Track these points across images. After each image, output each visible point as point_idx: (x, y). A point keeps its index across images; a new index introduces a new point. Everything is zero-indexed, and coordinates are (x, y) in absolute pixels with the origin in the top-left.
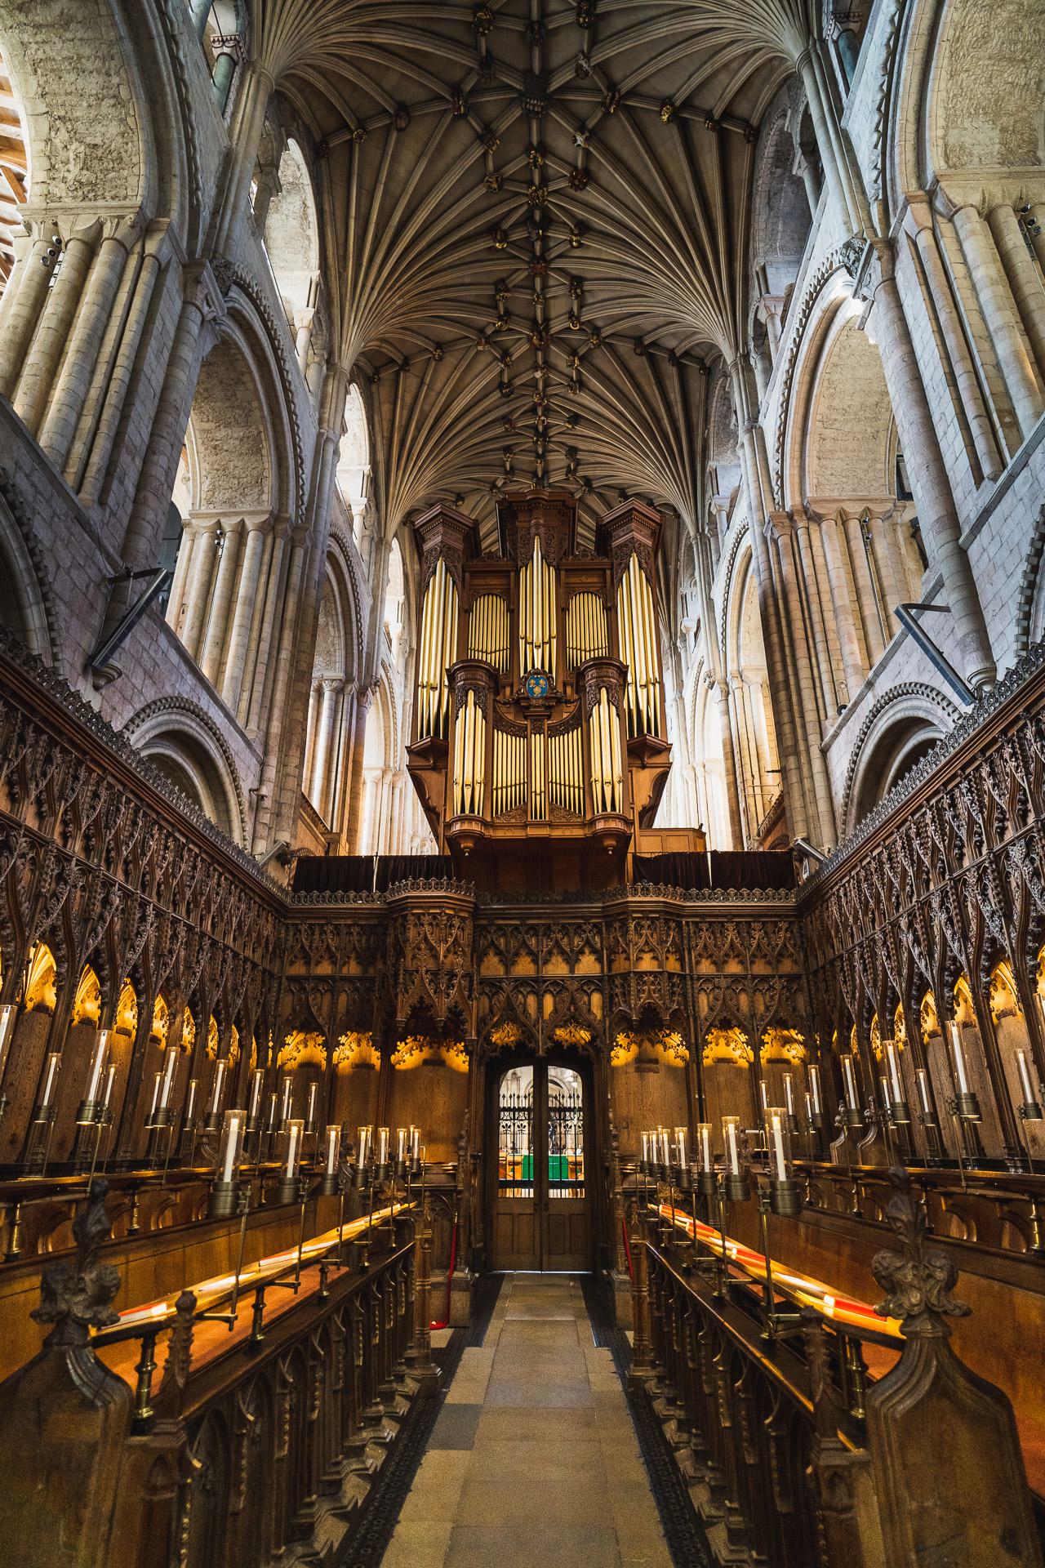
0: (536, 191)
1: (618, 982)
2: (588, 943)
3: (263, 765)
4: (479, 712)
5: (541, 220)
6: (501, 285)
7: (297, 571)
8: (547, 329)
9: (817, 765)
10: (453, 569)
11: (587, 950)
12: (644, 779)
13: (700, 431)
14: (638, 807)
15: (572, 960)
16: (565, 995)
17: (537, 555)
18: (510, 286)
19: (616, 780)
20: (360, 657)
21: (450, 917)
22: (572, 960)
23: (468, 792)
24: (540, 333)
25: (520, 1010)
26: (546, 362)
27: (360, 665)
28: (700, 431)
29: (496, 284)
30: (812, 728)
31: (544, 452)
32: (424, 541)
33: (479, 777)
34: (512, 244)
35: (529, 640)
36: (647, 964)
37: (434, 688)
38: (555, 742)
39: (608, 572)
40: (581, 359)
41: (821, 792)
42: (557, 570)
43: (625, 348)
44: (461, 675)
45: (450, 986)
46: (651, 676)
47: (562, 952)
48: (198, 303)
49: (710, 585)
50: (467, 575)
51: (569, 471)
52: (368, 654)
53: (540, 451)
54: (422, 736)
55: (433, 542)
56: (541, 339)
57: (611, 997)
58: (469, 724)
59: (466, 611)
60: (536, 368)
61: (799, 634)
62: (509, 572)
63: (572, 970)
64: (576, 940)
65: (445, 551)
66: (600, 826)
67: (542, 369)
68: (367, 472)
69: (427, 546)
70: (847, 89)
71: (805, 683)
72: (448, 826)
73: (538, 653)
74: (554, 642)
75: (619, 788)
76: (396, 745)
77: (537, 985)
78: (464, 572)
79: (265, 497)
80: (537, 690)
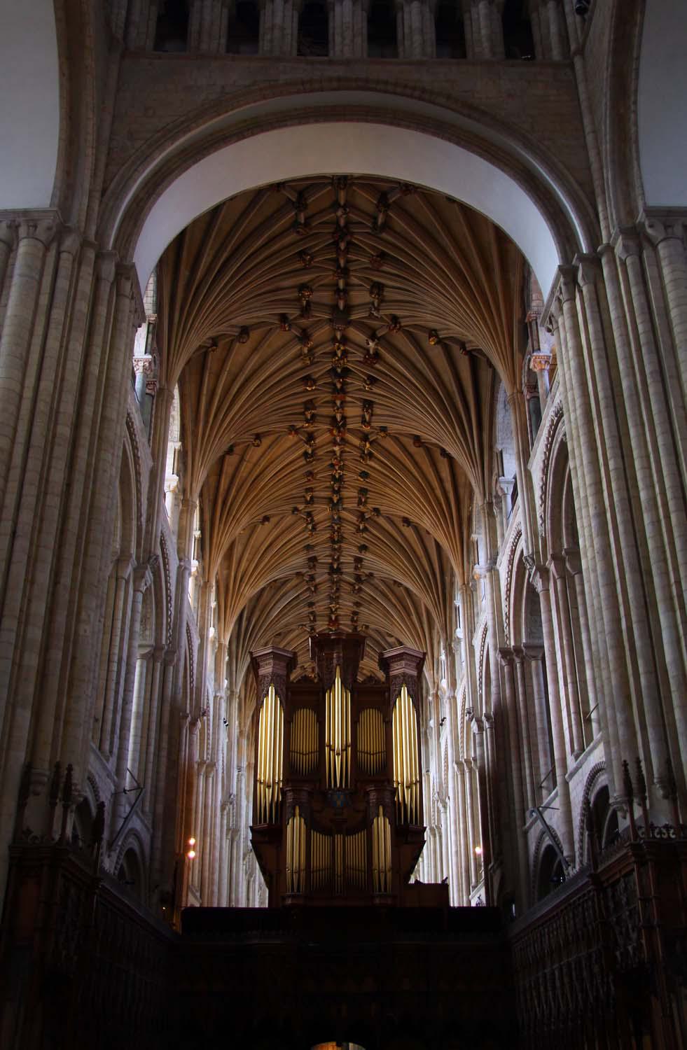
0: (338, 360)
3: (153, 838)
4: (303, 820)
5: (341, 339)
6: (309, 405)
7: (170, 685)
8: (344, 425)
13: (466, 506)
17: (338, 682)
18: (316, 405)
19: (387, 869)
24: (338, 428)
26: (342, 439)
27: (191, 700)
28: (466, 506)
29: (305, 403)
31: (339, 489)
32: (259, 667)
33: (303, 867)
34: (319, 385)
35: (332, 748)
37: (269, 787)
38: (349, 839)
39: (387, 694)
40: (371, 443)
43: (409, 442)
44: (289, 794)
46: (414, 779)
48: (141, 589)
49: (472, 633)
50: (289, 694)
51: (360, 503)
52: (197, 688)
53: (336, 489)
54: (260, 822)
55: (267, 669)
56: (339, 432)
58: (295, 828)
59: (288, 722)
60: (335, 443)
65: (275, 679)
66: (377, 901)
67: (339, 445)
68: (177, 448)
69: (262, 672)
70: (533, 444)
71: (515, 781)
72: (284, 899)
73: (338, 759)
75: (389, 875)
76: (208, 739)
79: (147, 633)
80: (339, 803)
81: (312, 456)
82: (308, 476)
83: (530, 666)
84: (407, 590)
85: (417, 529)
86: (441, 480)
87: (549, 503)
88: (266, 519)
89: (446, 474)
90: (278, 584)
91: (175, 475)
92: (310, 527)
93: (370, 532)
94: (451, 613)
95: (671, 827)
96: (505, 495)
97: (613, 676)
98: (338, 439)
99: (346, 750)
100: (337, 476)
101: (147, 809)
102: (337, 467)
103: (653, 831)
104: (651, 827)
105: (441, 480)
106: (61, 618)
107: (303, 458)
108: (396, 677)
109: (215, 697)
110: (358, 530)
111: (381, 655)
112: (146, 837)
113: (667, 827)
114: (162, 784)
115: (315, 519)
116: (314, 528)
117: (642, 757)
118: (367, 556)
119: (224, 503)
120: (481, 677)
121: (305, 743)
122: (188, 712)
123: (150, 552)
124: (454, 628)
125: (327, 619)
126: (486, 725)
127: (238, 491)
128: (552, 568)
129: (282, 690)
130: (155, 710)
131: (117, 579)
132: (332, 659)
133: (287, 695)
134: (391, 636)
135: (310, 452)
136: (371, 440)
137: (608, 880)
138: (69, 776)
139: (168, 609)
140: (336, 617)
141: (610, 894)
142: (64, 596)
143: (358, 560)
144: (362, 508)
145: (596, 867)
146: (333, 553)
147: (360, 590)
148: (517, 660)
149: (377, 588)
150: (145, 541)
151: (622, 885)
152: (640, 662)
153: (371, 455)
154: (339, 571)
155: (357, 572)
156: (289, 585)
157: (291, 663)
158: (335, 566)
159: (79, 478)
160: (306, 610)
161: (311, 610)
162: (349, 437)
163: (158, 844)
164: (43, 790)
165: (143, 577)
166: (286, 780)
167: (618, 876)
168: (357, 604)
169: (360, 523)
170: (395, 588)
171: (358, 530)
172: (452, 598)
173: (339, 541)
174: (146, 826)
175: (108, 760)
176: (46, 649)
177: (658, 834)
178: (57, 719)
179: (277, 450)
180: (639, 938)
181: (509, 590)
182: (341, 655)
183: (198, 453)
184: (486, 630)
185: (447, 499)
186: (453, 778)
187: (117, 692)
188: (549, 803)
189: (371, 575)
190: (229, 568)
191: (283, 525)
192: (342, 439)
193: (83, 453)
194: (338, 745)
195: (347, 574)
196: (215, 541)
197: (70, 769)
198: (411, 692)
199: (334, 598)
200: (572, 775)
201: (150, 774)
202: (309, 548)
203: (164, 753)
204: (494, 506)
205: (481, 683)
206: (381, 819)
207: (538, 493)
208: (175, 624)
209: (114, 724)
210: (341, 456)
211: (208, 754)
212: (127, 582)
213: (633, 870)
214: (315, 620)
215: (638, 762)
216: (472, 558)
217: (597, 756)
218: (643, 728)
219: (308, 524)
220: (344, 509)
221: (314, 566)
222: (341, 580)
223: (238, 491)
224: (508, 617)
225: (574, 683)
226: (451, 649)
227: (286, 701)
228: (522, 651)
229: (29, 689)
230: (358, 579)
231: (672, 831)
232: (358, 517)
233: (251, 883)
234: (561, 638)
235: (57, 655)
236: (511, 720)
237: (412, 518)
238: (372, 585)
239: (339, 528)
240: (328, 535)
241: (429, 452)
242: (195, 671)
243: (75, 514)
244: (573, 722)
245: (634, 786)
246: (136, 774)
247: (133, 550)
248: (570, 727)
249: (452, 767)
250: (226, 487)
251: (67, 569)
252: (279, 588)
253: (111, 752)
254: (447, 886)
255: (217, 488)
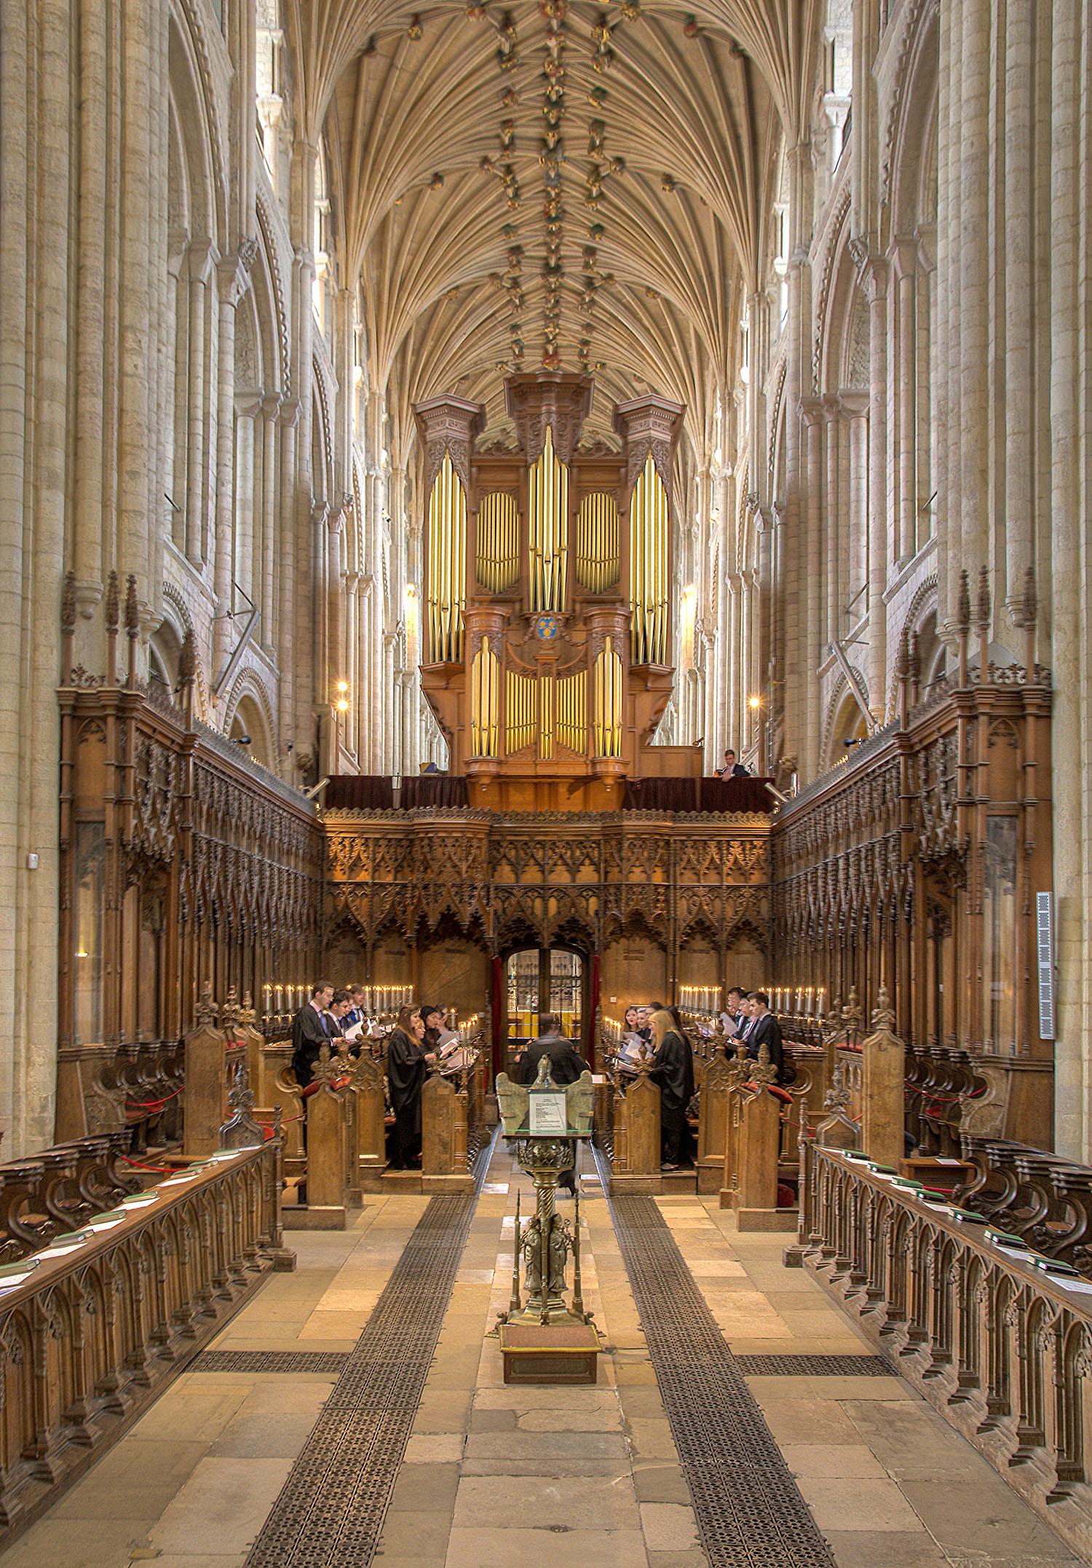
1: (612, 890)
2: (588, 856)
3: (280, 680)
4: (494, 658)
9: (811, 690)
10: (459, 467)
11: (587, 862)
12: (646, 701)
14: (639, 731)
15: (574, 870)
16: (567, 900)
17: (548, 450)
20: (329, 471)
21: (470, 840)
22: (574, 870)
23: (485, 735)
25: (529, 912)
26: (563, 24)
30: (810, 651)
36: (637, 876)
41: (811, 716)
42: (570, 467)
45: (471, 897)
47: (566, 864)
48: (232, 300)
50: (474, 470)
51: (593, 147)
53: (553, 121)
56: (557, 9)
57: (606, 902)
59: (473, 513)
60: (550, 32)
61: (812, 548)
62: (518, 467)
63: (574, 880)
64: (578, 853)
74: (564, 554)
75: (617, 733)
76: (360, 540)
77: (543, 891)
78: (471, 466)
81: (509, 60)
82: (505, 97)
83: (848, 427)
84: (667, 302)
85: (685, 195)
86: (728, 104)
87: (901, 141)
88: (438, 178)
89: (737, 91)
90: (461, 294)
91: (276, 96)
92: (510, 192)
93: (611, 203)
94: (734, 342)
95: (1021, 669)
96: (831, 127)
97: (964, 439)
98: (555, 23)
99: (559, 555)
100: (554, 98)
101: (269, 642)
102: (553, 80)
103: (992, 674)
104: (992, 667)
105: (728, 104)
106: (93, 344)
107: (495, 62)
108: (637, 443)
109: (368, 477)
110: (590, 198)
111: (616, 407)
112: (269, 681)
113: (1014, 668)
114: (289, 606)
115: (518, 178)
116: (516, 195)
117: (991, 565)
118: (602, 243)
119: (366, 147)
120: (773, 445)
121: (500, 543)
122: (325, 499)
123: (241, 236)
124: (737, 367)
125: (541, 352)
126: (777, 520)
127: (388, 126)
128: (894, 260)
129: (462, 463)
130: (271, 496)
131: (191, 283)
132: (539, 415)
133: (470, 473)
134: (640, 380)
135: (506, 49)
136: (611, 24)
137: (921, 741)
138: (131, 590)
139: (280, 335)
140: (556, 348)
141: (922, 761)
142: (94, 308)
143: (590, 251)
144: (596, 157)
145: (907, 724)
146: (548, 239)
147: (593, 301)
148: (828, 417)
149: (619, 301)
150: (230, 215)
151: (940, 747)
152: (1009, 415)
153: (610, 53)
154: (557, 270)
155: (588, 273)
156: (479, 296)
157: (477, 422)
158: (553, 263)
159: (93, 92)
160: (509, 337)
161: (514, 337)
162: (574, 19)
163: (288, 689)
164: (98, 612)
165: (232, 279)
166: (471, 601)
167: (935, 737)
168: (589, 327)
169: (593, 184)
170: (649, 300)
171: (590, 198)
172: (737, 318)
173: (557, 219)
174: (268, 666)
175: (200, 571)
176: (75, 395)
177: (1000, 677)
178: (105, 505)
179: (449, 46)
180: (953, 817)
181: (824, 301)
182: (554, 408)
183: (313, 51)
184: (784, 368)
185: (736, 138)
186: (724, 598)
187: (205, 467)
188: (856, 635)
189: (610, 277)
190: (381, 265)
191: (465, 191)
192: (563, 24)
193: (94, 44)
194: (548, 548)
195: (571, 275)
196: (353, 217)
197: (132, 581)
198: (661, 468)
199: (551, 318)
200: (892, 594)
201: (270, 590)
202: (508, 229)
203: (289, 560)
204: (813, 151)
205: (772, 454)
206: (609, 655)
207: (884, 121)
208: (294, 359)
209: (205, 516)
210: (560, 57)
211: (360, 562)
212: (207, 288)
213: (956, 728)
214: (521, 355)
215: (984, 573)
216: (771, 246)
217: (928, 568)
218: (1000, 520)
219: (508, 186)
220: (565, 159)
221: (519, 262)
222: (561, 286)
223: (388, 126)
224: (819, 346)
225: (911, 452)
226: (731, 400)
227: (470, 480)
228: (837, 402)
229: (58, 460)
230: (589, 283)
231: (1021, 673)
232: (590, 174)
233: (435, 745)
234: (896, 380)
235: (93, 405)
236: (812, 512)
237: (679, 176)
238: (612, 294)
239: (558, 195)
240: (540, 208)
241: (709, 45)
242: (332, 436)
243: (95, 162)
244: (902, 515)
245: (974, 608)
246: (248, 590)
247: (212, 233)
248: (897, 521)
249: (723, 584)
250: (367, 120)
251: (95, 260)
252: (462, 302)
253: (204, 558)
254: (702, 748)
255: (353, 119)
